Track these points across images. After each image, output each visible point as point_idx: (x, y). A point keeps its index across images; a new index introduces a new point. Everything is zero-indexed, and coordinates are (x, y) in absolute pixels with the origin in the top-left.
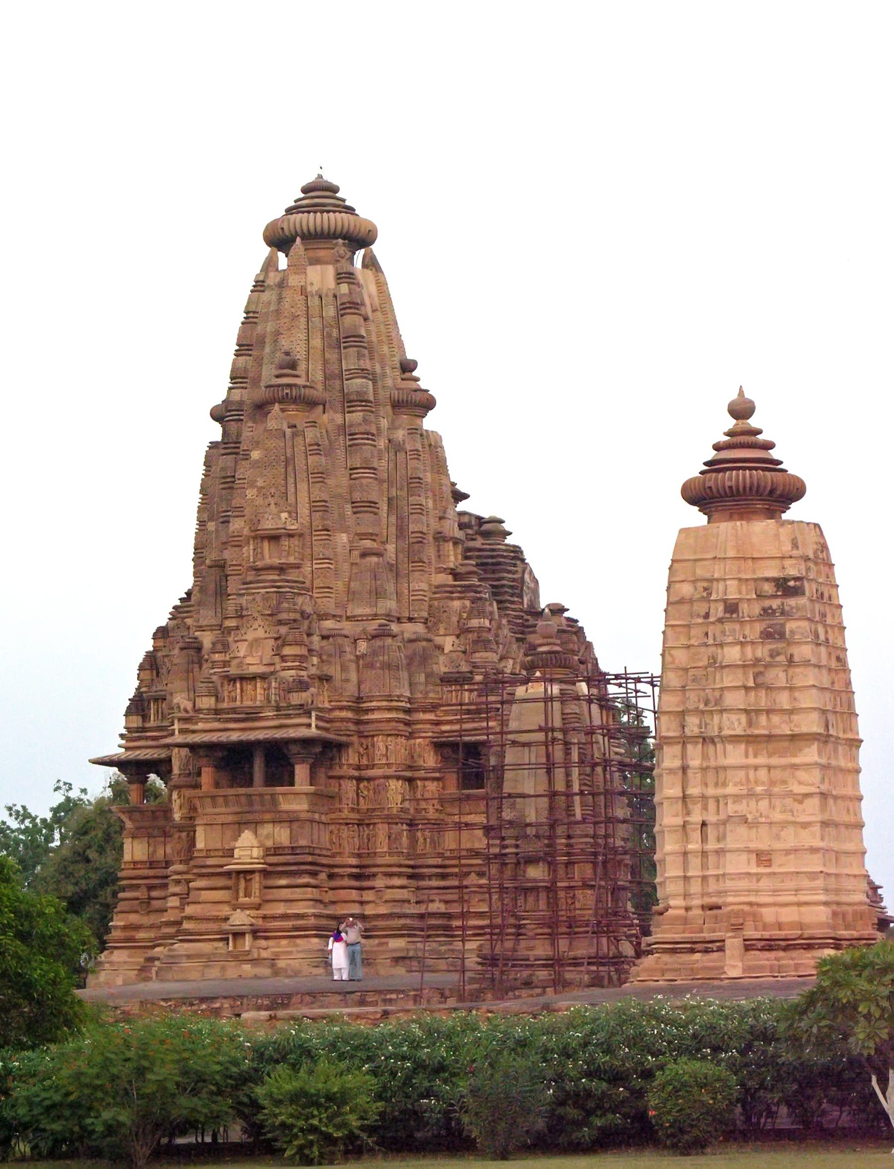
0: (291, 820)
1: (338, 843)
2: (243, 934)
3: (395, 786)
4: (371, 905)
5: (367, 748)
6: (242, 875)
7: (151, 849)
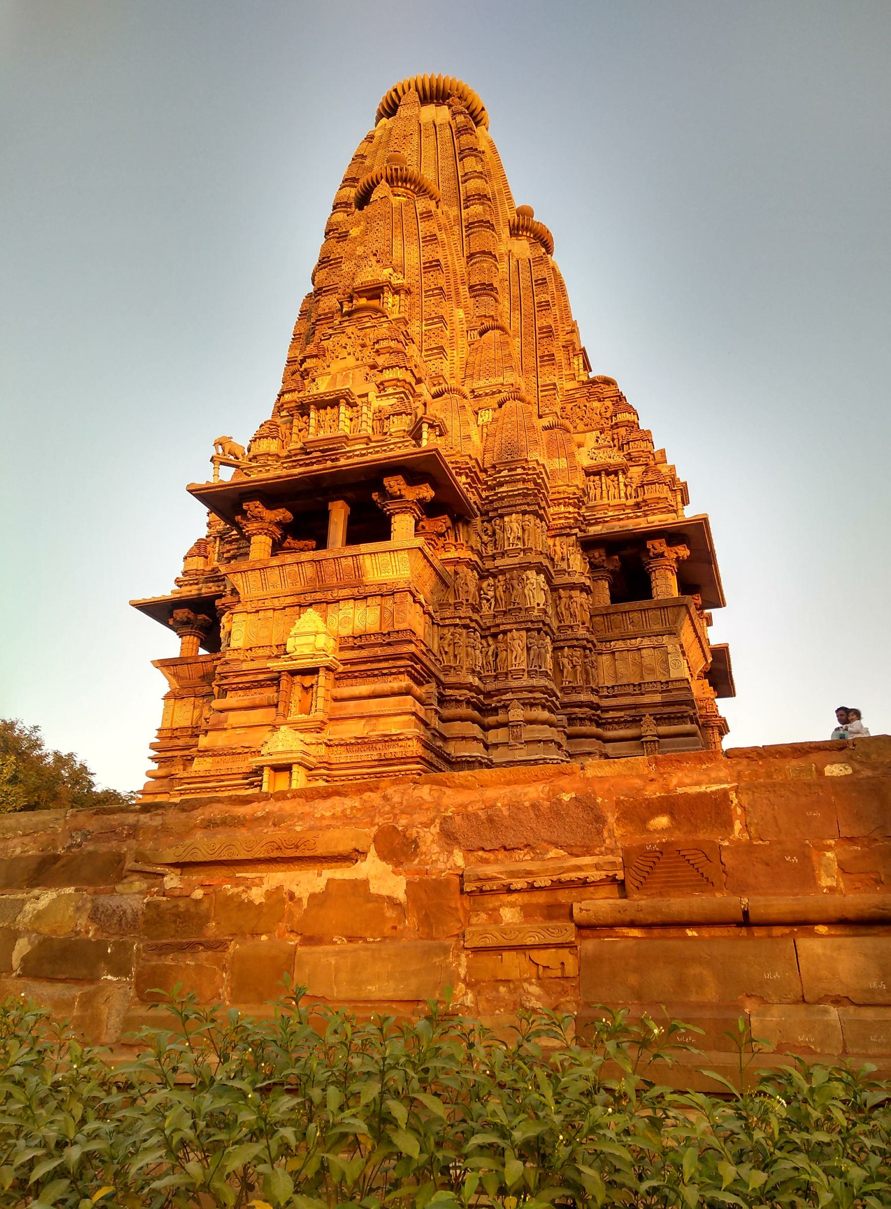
0: (387, 593)
1: (451, 653)
2: (287, 768)
3: (535, 579)
4: (501, 749)
5: (494, 533)
6: (298, 678)
7: (197, 713)
